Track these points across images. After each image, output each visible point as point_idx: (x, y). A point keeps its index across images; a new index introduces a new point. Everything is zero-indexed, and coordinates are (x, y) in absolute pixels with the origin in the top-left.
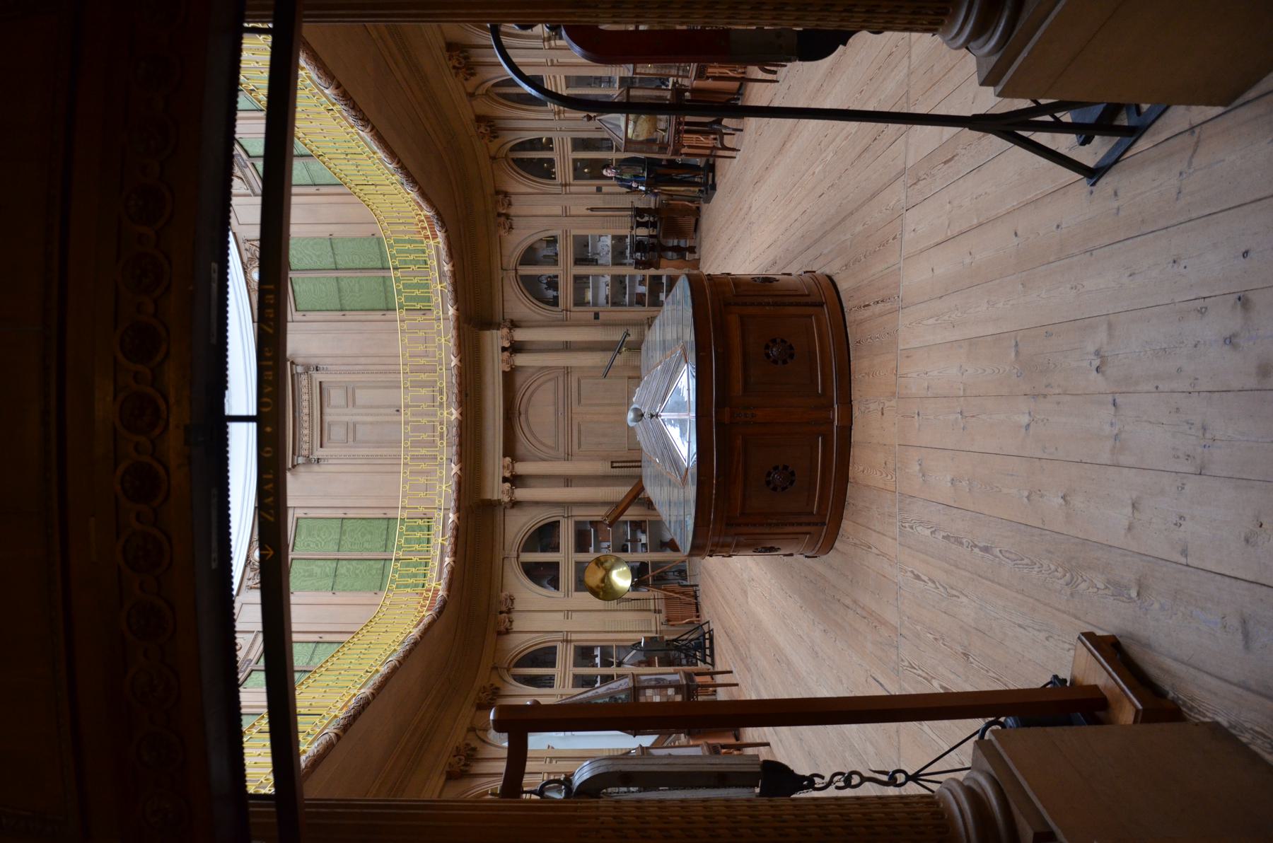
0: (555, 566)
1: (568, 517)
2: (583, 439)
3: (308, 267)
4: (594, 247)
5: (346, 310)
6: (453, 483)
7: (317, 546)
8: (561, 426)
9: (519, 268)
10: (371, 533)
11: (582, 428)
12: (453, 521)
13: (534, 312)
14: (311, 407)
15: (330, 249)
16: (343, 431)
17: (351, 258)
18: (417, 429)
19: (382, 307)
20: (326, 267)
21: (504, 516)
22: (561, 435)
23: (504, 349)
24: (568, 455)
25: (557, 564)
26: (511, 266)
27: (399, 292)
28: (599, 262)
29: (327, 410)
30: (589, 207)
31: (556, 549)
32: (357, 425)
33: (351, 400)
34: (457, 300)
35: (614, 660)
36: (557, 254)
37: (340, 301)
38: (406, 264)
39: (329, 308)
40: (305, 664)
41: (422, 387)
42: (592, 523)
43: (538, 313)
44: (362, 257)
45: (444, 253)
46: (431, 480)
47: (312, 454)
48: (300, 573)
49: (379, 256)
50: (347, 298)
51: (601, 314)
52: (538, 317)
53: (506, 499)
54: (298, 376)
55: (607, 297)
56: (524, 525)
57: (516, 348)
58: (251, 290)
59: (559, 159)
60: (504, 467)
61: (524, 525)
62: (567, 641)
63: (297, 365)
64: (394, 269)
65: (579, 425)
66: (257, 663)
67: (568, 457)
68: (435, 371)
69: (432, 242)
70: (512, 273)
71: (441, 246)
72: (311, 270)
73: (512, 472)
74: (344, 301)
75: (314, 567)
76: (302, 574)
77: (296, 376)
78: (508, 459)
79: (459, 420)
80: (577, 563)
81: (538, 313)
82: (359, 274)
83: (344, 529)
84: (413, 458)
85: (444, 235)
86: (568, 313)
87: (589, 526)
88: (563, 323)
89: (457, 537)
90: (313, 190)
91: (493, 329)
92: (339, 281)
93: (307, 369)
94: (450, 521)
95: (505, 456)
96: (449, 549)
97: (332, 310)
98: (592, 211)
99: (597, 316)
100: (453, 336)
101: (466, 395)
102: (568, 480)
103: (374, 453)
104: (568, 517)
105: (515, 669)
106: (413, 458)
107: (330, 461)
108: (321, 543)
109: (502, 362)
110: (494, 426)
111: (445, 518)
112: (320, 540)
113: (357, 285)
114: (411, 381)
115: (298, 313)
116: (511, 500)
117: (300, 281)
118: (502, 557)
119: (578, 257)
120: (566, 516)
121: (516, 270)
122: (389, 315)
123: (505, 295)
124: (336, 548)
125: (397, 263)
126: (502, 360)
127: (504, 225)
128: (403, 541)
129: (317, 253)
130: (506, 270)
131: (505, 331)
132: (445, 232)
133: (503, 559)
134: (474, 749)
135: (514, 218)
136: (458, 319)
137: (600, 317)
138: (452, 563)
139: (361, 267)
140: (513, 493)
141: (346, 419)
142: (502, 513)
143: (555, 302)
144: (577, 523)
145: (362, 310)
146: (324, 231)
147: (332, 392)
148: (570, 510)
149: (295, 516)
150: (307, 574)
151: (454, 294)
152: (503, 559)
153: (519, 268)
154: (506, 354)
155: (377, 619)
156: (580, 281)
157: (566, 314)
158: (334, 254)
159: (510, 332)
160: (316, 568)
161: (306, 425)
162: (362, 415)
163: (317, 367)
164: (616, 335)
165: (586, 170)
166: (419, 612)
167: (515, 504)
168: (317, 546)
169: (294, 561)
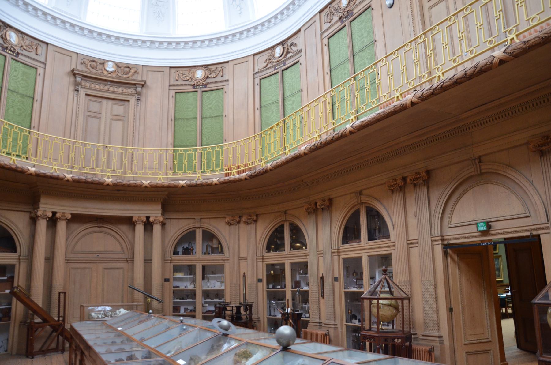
1: (19, 259)
2: (79, 271)
3: (204, 102)
4: (215, 278)
5: (175, 122)
6: (58, 174)
8: (90, 256)
9: (201, 230)
10: (20, 115)
11: (87, 271)
12: (29, 170)
13: (171, 239)
15: (216, 115)
16: (95, 110)
19: (175, 143)
20: (203, 112)
22: (83, 255)
23: (148, 218)
24: (68, 260)
26: (202, 224)
28: (203, 281)
29: (110, 102)
30: (246, 274)
32: (98, 119)
33: (116, 118)
34: (190, 186)
36: (209, 254)
37: (181, 119)
39: (176, 112)
42: (12, 278)
43: (169, 242)
47: (81, 87)
49: (210, 143)
51: (168, 283)
52: (167, 241)
53: (39, 213)
54: (135, 88)
55: (178, 287)
56: (15, 225)
58: (190, 68)
59: (285, 254)
60: (64, 213)
61: (15, 225)
63: (142, 88)
65: (89, 268)
67: (68, 261)
70: (198, 225)
72: (202, 103)
73: (60, 218)
74: (180, 121)
77: (135, 86)
78: (69, 217)
79: (104, 183)
81: (169, 242)
82: (198, 131)
83: (26, 97)
88: (164, 259)
90: (257, 105)
91: (162, 211)
92: (194, 119)
93: (139, 94)
94: (29, 168)
95: (72, 214)
97: (175, 113)
98: (243, 276)
99: (167, 280)
100: (163, 182)
101: (119, 190)
103: (79, 127)
107: (75, 98)
108: (17, 79)
110: (94, 208)
116: (38, 217)
120: (21, 258)
121: (199, 228)
123: (182, 220)
124: (11, 89)
126: (140, 216)
127: (232, 220)
128: (16, 130)
129: (213, 108)
130: (200, 221)
131: (161, 219)
136: (176, 187)
140: (44, 219)
141: (104, 113)
142: (26, 210)
143: (176, 253)
144: (13, 267)
145: (174, 131)
146: (228, 111)
148: (24, 261)
151: (195, 184)
153: (201, 230)
154: (145, 219)
156: (191, 269)
157: (169, 260)
159: (160, 222)
161: (102, 87)
162: (105, 123)
163: (139, 100)
164: (156, 293)
165: (272, 272)
167: (34, 220)
168: (15, 76)
169: (3, 57)
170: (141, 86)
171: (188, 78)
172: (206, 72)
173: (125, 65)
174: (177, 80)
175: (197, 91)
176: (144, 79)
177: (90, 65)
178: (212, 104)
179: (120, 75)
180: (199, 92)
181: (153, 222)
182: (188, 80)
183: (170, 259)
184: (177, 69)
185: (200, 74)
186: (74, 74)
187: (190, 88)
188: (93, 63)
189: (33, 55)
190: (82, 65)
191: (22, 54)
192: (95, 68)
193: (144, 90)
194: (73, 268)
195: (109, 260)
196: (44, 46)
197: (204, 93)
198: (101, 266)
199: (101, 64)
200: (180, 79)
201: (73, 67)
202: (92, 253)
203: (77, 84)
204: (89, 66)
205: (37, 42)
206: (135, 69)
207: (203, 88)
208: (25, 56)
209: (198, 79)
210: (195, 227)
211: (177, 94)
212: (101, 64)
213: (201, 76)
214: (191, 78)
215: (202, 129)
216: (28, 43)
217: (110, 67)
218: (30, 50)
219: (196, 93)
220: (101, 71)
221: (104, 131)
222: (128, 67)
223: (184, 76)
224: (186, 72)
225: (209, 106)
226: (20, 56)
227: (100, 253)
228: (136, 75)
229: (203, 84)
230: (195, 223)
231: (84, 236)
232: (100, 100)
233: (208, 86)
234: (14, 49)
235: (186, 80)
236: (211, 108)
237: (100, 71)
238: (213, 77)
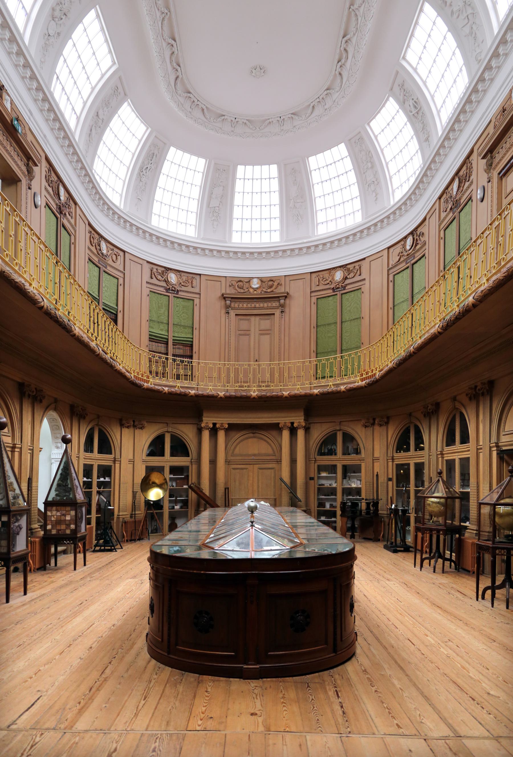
1: (191, 462)
2: (238, 471)
14: (260, 308)
15: (354, 317)
20: (343, 316)
22: (240, 458)
27: (328, 360)
29: (258, 318)
33: (264, 332)
34: (323, 395)
37: (323, 325)
38: (345, 364)
40: (103, 301)
41: (270, 375)
42: (187, 476)
45: (352, 386)
48: (161, 300)
63: (285, 300)
64: (341, 356)
65: (246, 469)
66: (104, 271)
67: (228, 462)
68: (280, 382)
69: (358, 378)
71: (357, 384)
74: (322, 327)
76: (160, 302)
82: (338, 336)
84: (228, 369)
85: (363, 385)
87: (185, 474)
93: (282, 306)
102: (214, 462)
104: (191, 462)
106: (228, 369)
107: (227, 320)
114: (274, 368)
115: (316, 300)
122: (313, 355)
125: (346, 358)
134: (41, 401)
145: (317, 338)
150: (160, 305)
155: (130, 344)
158: (351, 320)
160: (163, 310)
161: (249, 305)
166: (134, 371)
173: (269, 279)
174: (318, 285)
175: (336, 295)
176: (287, 290)
179: (264, 290)
180: (338, 295)
186: (225, 298)
188: (240, 283)
190: (231, 288)
191: (181, 291)
192: (242, 288)
193: (287, 301)
194: (234, 469)
196: (199, 276)
197: (343, 296)
199: (247, 282)
200: (320, 284)
201: (223, 291)
204: (236, 287)
205: (192, 275)
206: (279, 281)
208: (183, 291)
212: (247, 282)
216: (184, 278)
217: (255, 284)
222: (272, 280)
223: (325, 280)
225: (349, 309)
228: (280, 287)
231: (242, 441)
232: (248, 317)
234: (175, 288)
236: (350, 311)
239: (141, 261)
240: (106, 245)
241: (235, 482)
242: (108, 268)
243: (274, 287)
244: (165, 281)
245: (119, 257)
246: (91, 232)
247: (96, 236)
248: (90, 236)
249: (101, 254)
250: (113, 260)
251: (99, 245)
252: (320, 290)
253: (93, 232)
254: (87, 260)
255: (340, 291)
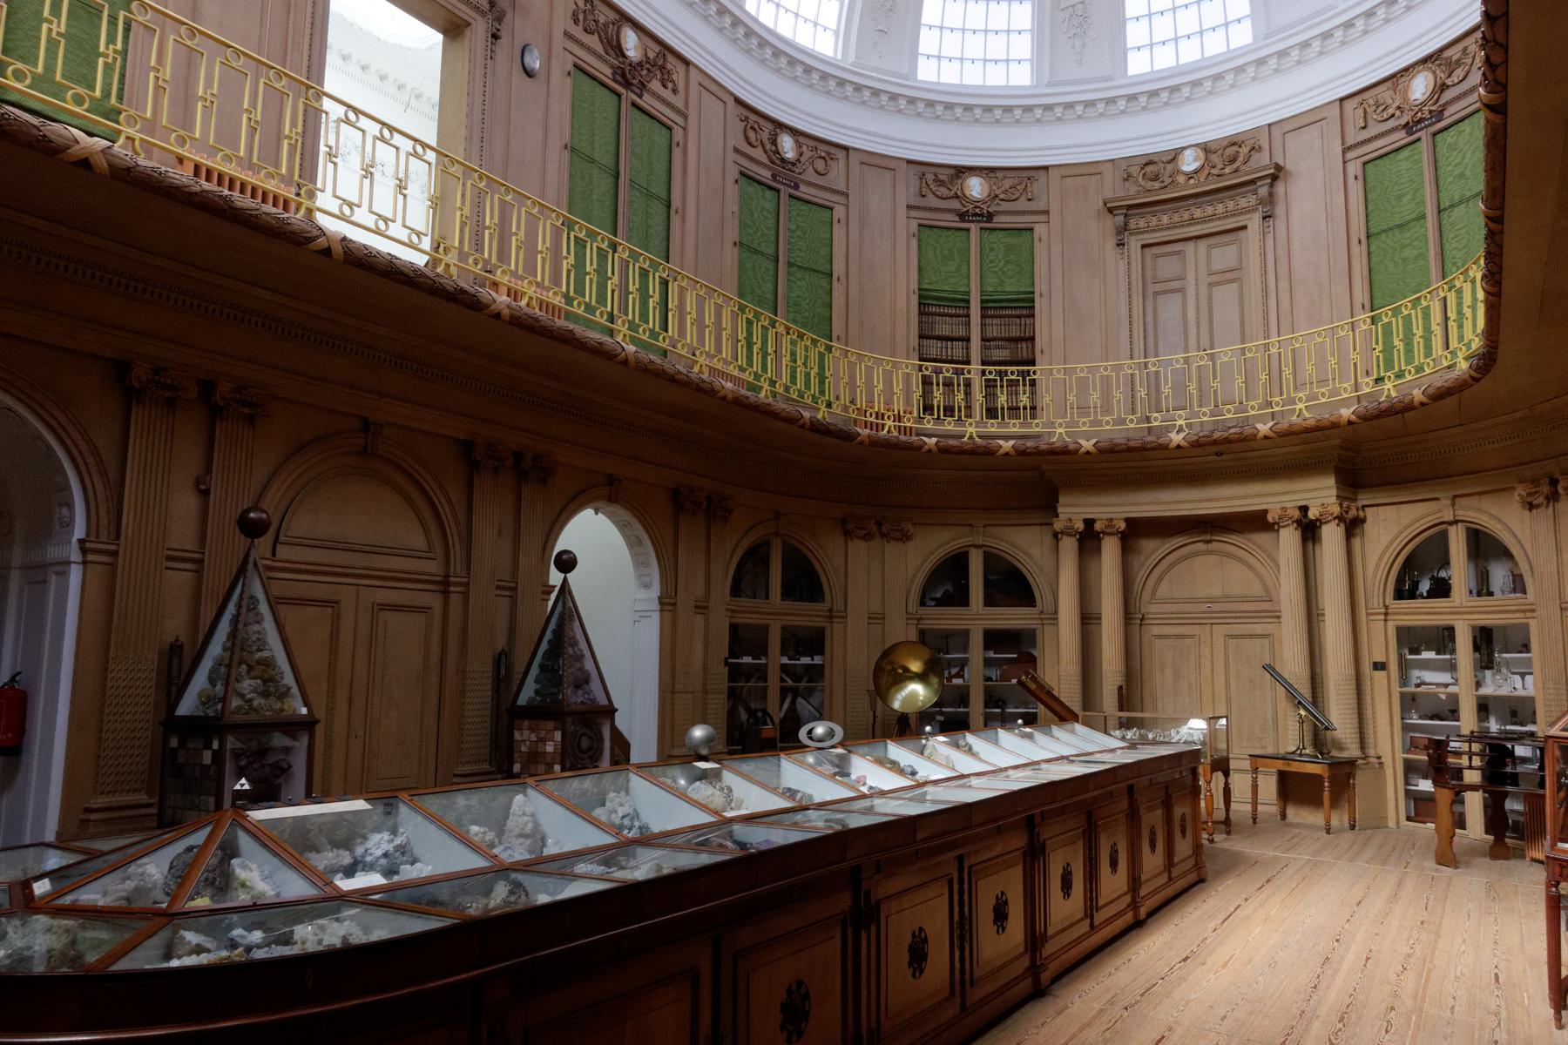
0: (963, 601)
2: (1170, 642)
7: (992, 262)
8: (1188, 607)
17: (1461, 232)
18: (1155, 383)
21: (1041, 524)
25: (967, 604)
31: (989, 601)
35: (804, 684)
36: (1491, 594)
37: (1384, 231)
43: (1377, 566)
44: (1464, 251)
46: (1095, 412)
47: (1131, 234)
50: (1389, 242)
51: (1382, 674)
52: (1371, 566)
57: (1309, 530)
58: (1395, 80)
62: (831, 616)
65: (1192, 636)
70: (1448, 516)
73: (1103, 532)
75: (958, 261)
78: (1123, 525)
80: (966, 633)
86: (1382, 617)
89: (975, 452)
93: (1271, 199)
95: (1128, 521)
96: (952, 442)
97: (1367, 222)
105: (780, 547)
106: (1106, 381)
109: (1283, 508)
111: (1006, 438)
112: (1001, 265)
113: (1415, 252)
117: (1415, 157)
118: (972, 522)
119: (1495, 636)
121: (1456, 522)
129: (1468, 173)
130: (1453, 505)
131: (1336, 510)
132: (1472, 377)
133: (971, 525)
135: (1550, 509)
137: (1377, 672)
138: (926, 447)
139: (1447, 252)
140: (1069, 535)
141: (1191, 276)
147: (1233, 248)
149: (1037, 225)
151: (1376, 412)
152: (971, 525)
154: (1296, 514)
156: (1443, 639)
161: (1176, 218)
170: (1269, 181)
171: (1391, 111)
172: (1438, 72)
173: (1225, 143)
174: (1364, 128)
175: (1419, 140)
177: (1144, 174)
178: (1466, 161)
179: (1214, 171)
180: (1424, 138)
181: (1317, 520)
182: (1393, 116)
183: (1383, 610)
184: (1358, 99)
185: (1420, 87)
186: (1110, 210)
187: (1400, 137)
189: (1022, 205)
192: (1156, 178)
193: (1280, 188)
195: (1236, 618)
196: (1042, 173)
197: (1439, 137)
198: (1220, 631)
200: (1370, 122)
201: (1109, 195)
202: (1196, 601)
203: (1124, 229)
207: (1430, 125)
209: (1417, 102)
210: (1442, 523)
211: (1370, 165)
213: (1424, 91)
214: (1399, 108)
215: (1442, 244)
216: (1007, 184)
217: (1189, 163)
218: (1014, 197)
219: (1417, 144)
220: (1171, 179)
221: (1198, 318)
222: (1234, 142)
224: (1384, 94)
226: (996, 219)
227: (1213, 600)
228: (1256, 156)
229: (1430, 112)
230: (1440, 511)
233: (1446, 114)
235: (1387, 120)
236: (1462, 175)
237: (1168, 181)
238: (1456, 81)
239: (892, 164)
240: (797, 142)
241: (1162, 670)
242: (803, 188)
243: (1241, 159)
244: (958, 197)
245: (830, 162)
246: (747, 118)
247: (770, 126)
248: (746, 126)
249: (778, 162)
250: (816, 171)
251: (774, 142)
252: (1369, 140)
253: (753, 117)
254: (732, 173)
255: (1427, 127)
